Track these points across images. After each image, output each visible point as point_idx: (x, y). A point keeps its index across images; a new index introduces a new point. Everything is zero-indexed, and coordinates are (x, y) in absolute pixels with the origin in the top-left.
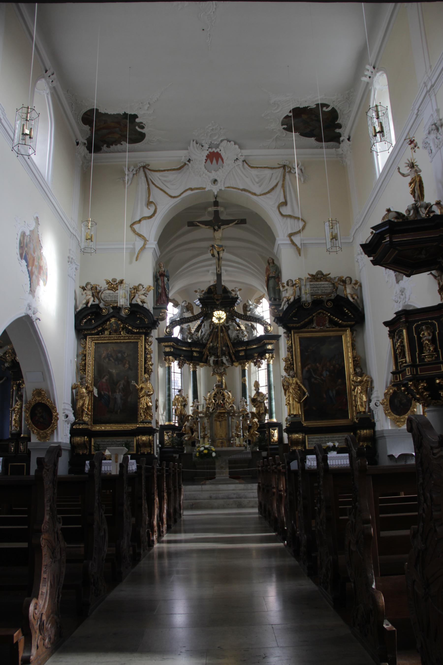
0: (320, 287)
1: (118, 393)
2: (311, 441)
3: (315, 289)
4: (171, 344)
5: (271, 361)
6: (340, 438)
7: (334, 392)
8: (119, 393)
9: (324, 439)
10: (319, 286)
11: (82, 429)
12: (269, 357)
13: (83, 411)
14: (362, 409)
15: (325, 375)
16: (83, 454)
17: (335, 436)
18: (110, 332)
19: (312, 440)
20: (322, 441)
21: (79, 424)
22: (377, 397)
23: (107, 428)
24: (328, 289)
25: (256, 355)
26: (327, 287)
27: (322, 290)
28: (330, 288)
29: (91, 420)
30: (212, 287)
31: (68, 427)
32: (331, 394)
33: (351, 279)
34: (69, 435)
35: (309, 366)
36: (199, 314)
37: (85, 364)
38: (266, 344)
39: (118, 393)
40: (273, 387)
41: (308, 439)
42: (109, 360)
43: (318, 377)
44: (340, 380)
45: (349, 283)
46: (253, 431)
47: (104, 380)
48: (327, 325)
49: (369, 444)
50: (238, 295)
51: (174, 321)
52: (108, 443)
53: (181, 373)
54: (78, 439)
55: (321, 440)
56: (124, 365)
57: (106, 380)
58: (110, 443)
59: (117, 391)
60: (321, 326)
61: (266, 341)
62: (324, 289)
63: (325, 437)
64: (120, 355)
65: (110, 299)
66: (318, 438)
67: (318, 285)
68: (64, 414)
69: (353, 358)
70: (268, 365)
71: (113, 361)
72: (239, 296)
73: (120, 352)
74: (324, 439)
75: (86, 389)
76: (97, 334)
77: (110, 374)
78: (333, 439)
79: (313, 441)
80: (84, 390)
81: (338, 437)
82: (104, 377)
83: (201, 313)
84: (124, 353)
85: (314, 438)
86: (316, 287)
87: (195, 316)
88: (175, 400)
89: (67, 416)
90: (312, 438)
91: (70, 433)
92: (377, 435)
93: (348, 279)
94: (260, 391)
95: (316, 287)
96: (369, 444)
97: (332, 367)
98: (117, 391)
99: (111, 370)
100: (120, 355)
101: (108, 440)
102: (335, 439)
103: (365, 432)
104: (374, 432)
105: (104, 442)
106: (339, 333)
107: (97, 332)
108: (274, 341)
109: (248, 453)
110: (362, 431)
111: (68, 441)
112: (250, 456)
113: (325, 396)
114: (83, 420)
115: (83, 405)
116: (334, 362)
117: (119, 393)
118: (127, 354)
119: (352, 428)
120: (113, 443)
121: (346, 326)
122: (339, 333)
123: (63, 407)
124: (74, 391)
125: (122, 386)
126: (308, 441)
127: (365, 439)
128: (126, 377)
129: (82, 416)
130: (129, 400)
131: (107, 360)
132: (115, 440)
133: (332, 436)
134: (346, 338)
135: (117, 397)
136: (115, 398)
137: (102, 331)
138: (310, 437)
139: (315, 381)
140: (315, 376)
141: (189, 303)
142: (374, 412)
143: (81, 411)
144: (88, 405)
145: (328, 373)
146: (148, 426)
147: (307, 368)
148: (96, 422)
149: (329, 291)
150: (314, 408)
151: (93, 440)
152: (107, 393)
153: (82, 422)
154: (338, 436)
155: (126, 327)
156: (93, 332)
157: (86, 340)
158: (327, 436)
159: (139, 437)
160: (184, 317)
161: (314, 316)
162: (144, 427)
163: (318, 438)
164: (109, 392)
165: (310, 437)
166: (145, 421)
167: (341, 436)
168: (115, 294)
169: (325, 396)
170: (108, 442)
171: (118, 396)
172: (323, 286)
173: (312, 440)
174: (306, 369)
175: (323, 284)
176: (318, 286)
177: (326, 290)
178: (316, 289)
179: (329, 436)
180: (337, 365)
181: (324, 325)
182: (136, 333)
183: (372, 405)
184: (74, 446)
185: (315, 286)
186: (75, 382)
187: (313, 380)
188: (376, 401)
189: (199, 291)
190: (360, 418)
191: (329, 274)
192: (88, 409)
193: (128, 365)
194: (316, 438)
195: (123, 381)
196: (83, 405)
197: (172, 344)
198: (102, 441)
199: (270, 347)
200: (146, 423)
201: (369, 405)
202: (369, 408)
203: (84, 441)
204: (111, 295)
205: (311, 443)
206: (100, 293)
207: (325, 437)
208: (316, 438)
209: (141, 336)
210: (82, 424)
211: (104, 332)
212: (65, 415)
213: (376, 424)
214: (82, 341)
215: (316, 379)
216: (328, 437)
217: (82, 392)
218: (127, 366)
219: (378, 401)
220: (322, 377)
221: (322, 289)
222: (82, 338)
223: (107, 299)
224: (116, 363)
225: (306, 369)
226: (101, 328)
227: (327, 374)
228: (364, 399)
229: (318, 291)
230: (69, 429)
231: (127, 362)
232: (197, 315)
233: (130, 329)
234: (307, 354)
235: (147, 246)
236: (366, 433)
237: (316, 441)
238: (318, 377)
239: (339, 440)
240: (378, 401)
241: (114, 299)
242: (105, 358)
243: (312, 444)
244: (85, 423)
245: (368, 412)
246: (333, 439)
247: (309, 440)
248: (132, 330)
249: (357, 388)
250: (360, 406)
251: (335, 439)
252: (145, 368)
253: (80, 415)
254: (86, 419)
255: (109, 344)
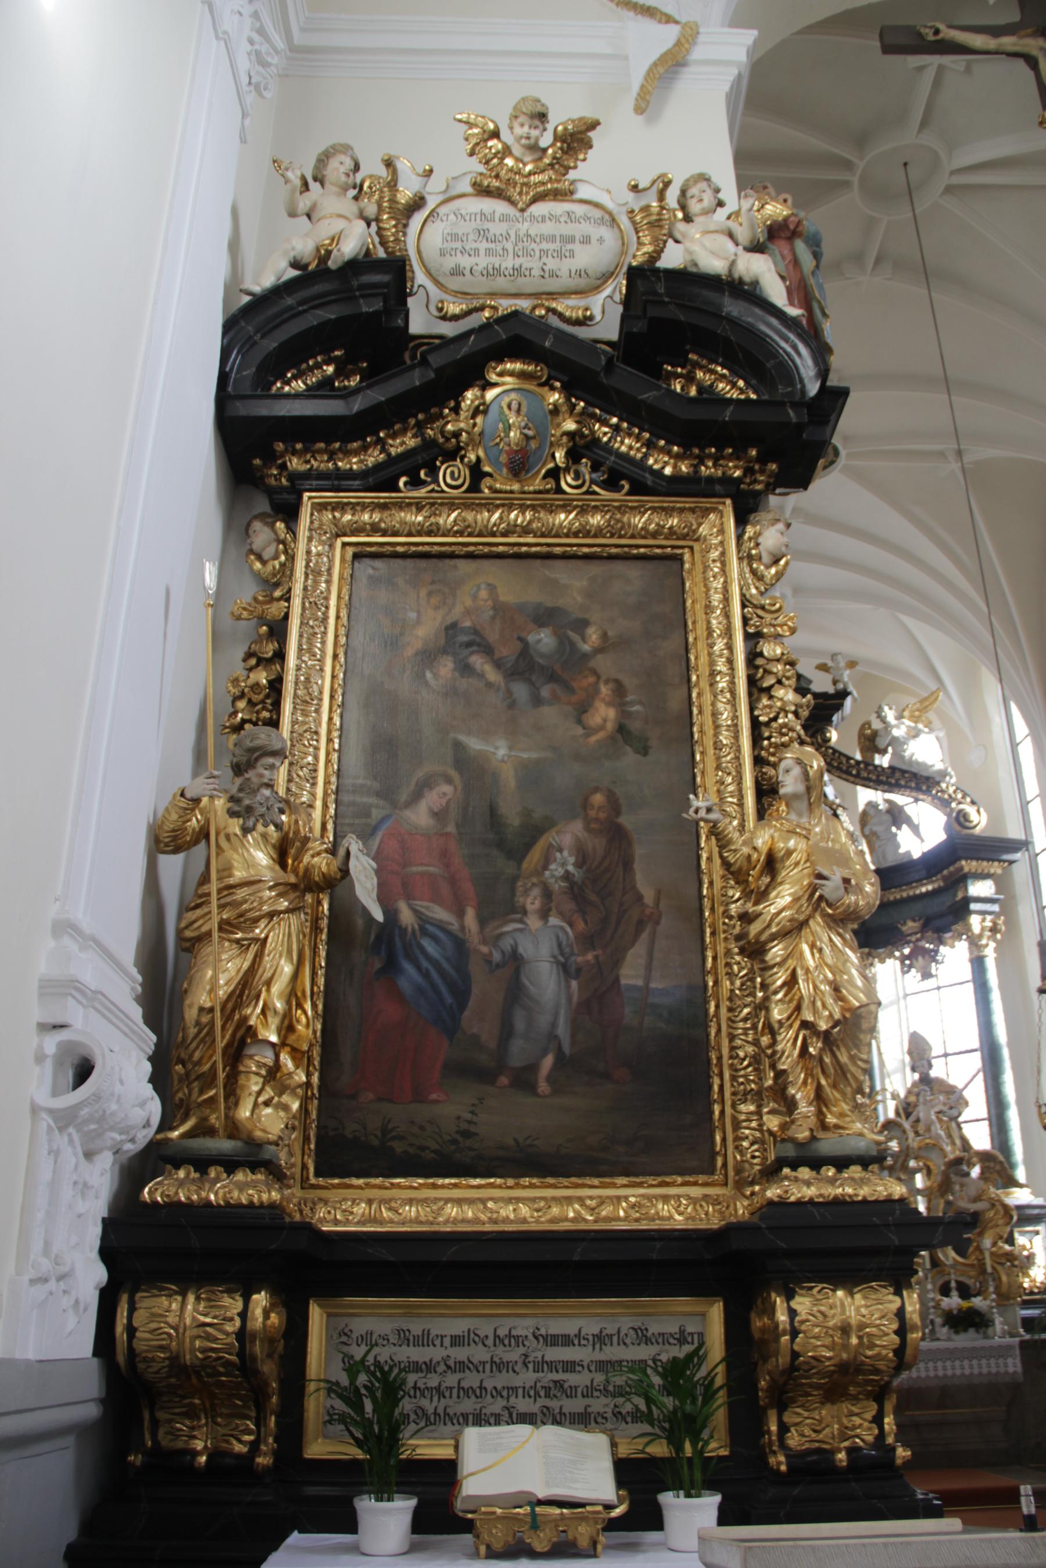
1: (534, 922)
5: (992, 945)
8: (544, 914)
11: (231, 1209)
12: (983, 929)
13: (244, 1037)
16: (228, 1469)
18: (477, 473)
21: (202, 1164)
23: (452, 1211)
25: (911, 926)
29: (306, 1139)
31: (84, 1188)
34: (100, 1274)
37: (276, 685)
38: (962, 879)
39: (534, 922)
40: (1006, 1053)
42: (465, 669)
46: (994, 1244)
47: (420, 816)
50: (845, 684)
52: (460, 1354)
54: (187, 1318)
56: (582, 709)
57: (439, 816)
58: (479, 1354)
59: (533, 902)
61: (968, 866)
64: (544, 639)
65: (483, 262)
68: (51, 1044)
70: (978, 963)
71: (492, 674)
72: (851, 688)
73: (544, 617)
75: (282, 853)
76: (381, 479)
77: (465, 764)
80: (262, 858)
82: (417, 796)
84: (581, 625)
89: (84, 1071)
91: (107, 1253)
94: (933, 1073)
98: (533, 902)
99: (474, 744)
100: (544, 639)
101: (458, 1326)
105: (425, 1340)
107: (378, 467)
108: (996, 868)
109: (1002, 1352)
111: (77, 1337)
112: (1014, 1365)
114: (233, 1129)
115: (246, 988)
117: (544, 914)
118: (604, 636)
120: (514, 1355)
123: (43, 967)
124: (171, 866)
125: (564, 864)
128: (598, 798)
129: (232, 1093)
130: (630, 974)
131: (446, 667)
132: (523, 1327)
135: (526, 948)
136: (515, 960)
137: (421, 464)
143: (220, 1044)
144: (293, 997)
146: (864, 1192)
148: (343, 1151)
151: (316, 1315)
152: (440, 914)
153: (224, 1145)
155: (596, 441)
156: (354, 464)
157: (292, 530)
159: (802, 1304)
162: (837, 1202)
164: (460, 914)
166: (828, 1145)
168: (524, 227)
170: (457, 1341)
171: (539, 941)
182: (677, 486)
184: (131, 1383)
186: (183, 777)
192: (287, 1028)
193: (611, 713)
195: (577, 827)
196: (246, 988)
198: (404, 1338)
199: (980, 888)
200: (842, 1163)
203: (242, 1334)
204: (497, 229)
206: (417, 220)
209: (706, 512)
210: (230, 1165)
211: (433, 471)
212: (65, 1049)
214: (262, 535)
217: (239, 874)
218: (604, 714)
222: (261, 517)
223: (466, 262)
224: (521, 691)
226: (411, 441)
230: (97, 1206)
231: (605, 690)
233: (625, 457)
235: (698, 53)
241: (509, 263)
242: (428, 657)
244: (253, 1156)
248: (641, 465)
252: (756, 725)
253: (208, 1080)
254: (267, 1114)
255: (464, 566)
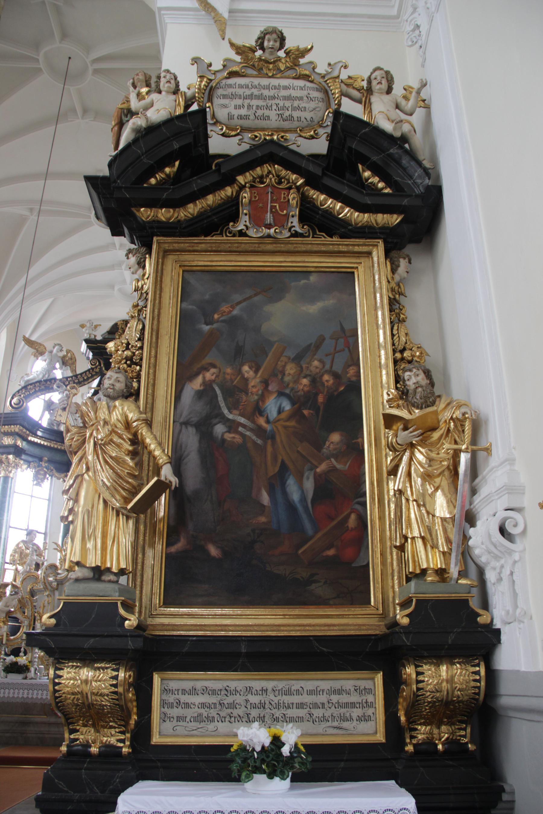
0: (274, 98)
2: (179, 703)
3: (255, 103)
4: (16, 428)
6: (323, 698)
7: (309, 485)
9: (239, 699)
10: (272, 93)
14: (428, 559)
15: (273, 413)
17: (296, 685)
19: (184, 698)
20: (232, 706)
22: (512, 489)
24: (303, 105)
26: (301, 99)
27: (284, 108)
28: (312, 105)
30: (119, 323)
32: (295, 497)
33: (389, 78)
35: (209, 375)
36: (85, 372)
41: (165, 691)
43: (242, 420)
44: (335, 437)
45: (384, 85)
48: (295, 222)
49: (465, 735)
51: (31, 384)
53: (49, 500)
55: (229, 700)
60: (269, 227)
62: (288, 104)
63: (249, 690)
66: (214, 692)
67: (268, 87)
69: (394, 351)
74: (239, 699)
78: (287, 699)
79: (187, 705)
81: (311, 693)
83: (89, 370)
85: (193, 691)
86: (260, 97)
87: (76, 376)
88: (15, 551)
90: (184, 692)
92: (508, 696)
93: (377, 73)
95: (259, 97)
96: (465, 735)
97: (305, 381)
102: (296, 699)
103: (441, 677)
104: (492, 676)
106: (344, 262)
110: (426, 668)
113: (265, 499)
116: (316, 363)
119: (382, 654)
121: (367, 232)
122: (344, 262)
126: (163, 703)
127: (446, 709)
133: (280, 685)
134: (372, 278)
138: (173, 685)
139: (228, 436)
140: (231, 417)
141: (68, 351)
142: (490, 576)
145: (287, 406)
147: (199, 380)
149: (308, 115)
150: (213, 551)
154: (309, 685)
158: (257, 685)
160: (51, 377)
161: (242, 187)
163: (214, 692)
165: (173, 685)
167: (325, 685)
169: (265, 499)
172: (283, 93)
173: (184, 698)
174: (197, 384)
175: (286, 88)
176: (266, 93)
177: (294, 109)
178: (261, 103)
179: (269, 685)
180: (326, 377)
181: (280, 221)
183: (482, 536)
185: (256, 92)
187: (219, 429)
188: (502, 514)
189: (88, 325)
190: (419, 602)
191: (308, 51)
194: (205, 691)
197: (17, 430)
201: (466, 538)
202: (466, 553)
205: (176, 712)
207: (249, 690)
208: (205, 691)
213: (503, 637)
215: (232, 426)
216: (264, 691)
219: (518, 510)
220: (262, 421)
221: (281, 103)
225: (197, 384)
227: (280, 411)
228: (441, 506)
229: (267, 112)
232: (81, 374)
234: (206, 328)
236: (450, 680)
237: (203, 705)
238: (242, 420)
239: (315, 706)
240: (518, 510)
243: (179, 719)
245: (463, 574)
246: (287, 699)
247: (171, 699)
249: (405, 458)
250: (419, 543)
251: (296, 699)
